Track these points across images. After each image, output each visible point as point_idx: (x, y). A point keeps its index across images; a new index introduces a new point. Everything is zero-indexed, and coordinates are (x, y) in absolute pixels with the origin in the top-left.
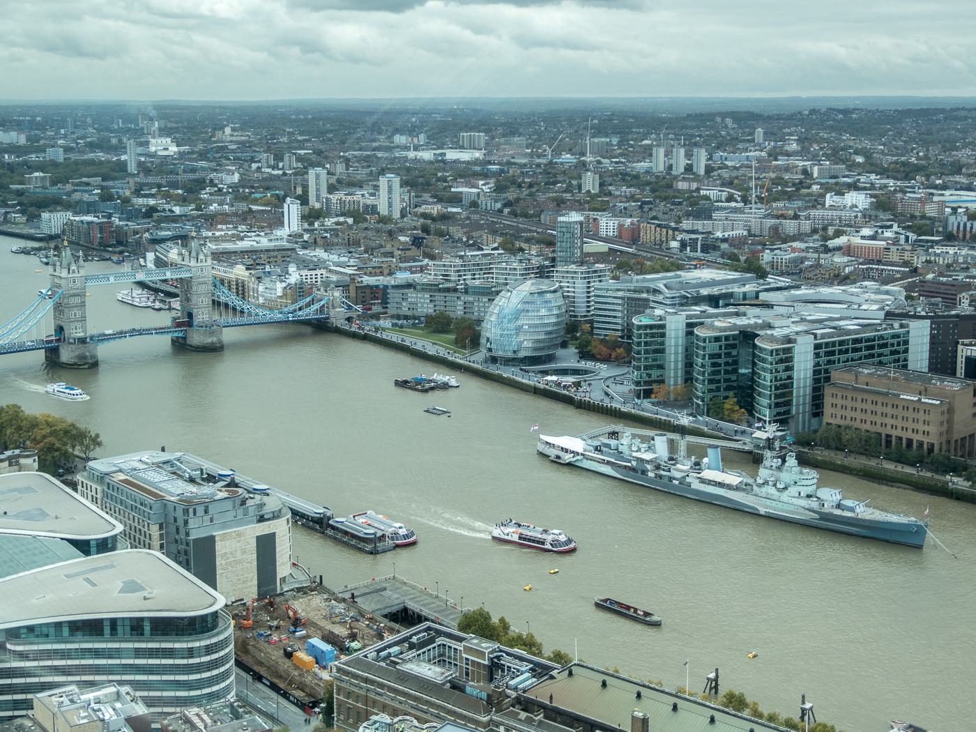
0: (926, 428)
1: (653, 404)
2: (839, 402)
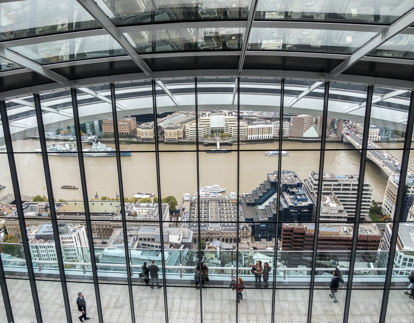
0: (126, 129)
1: (61, 135)
2: (106, 127)
